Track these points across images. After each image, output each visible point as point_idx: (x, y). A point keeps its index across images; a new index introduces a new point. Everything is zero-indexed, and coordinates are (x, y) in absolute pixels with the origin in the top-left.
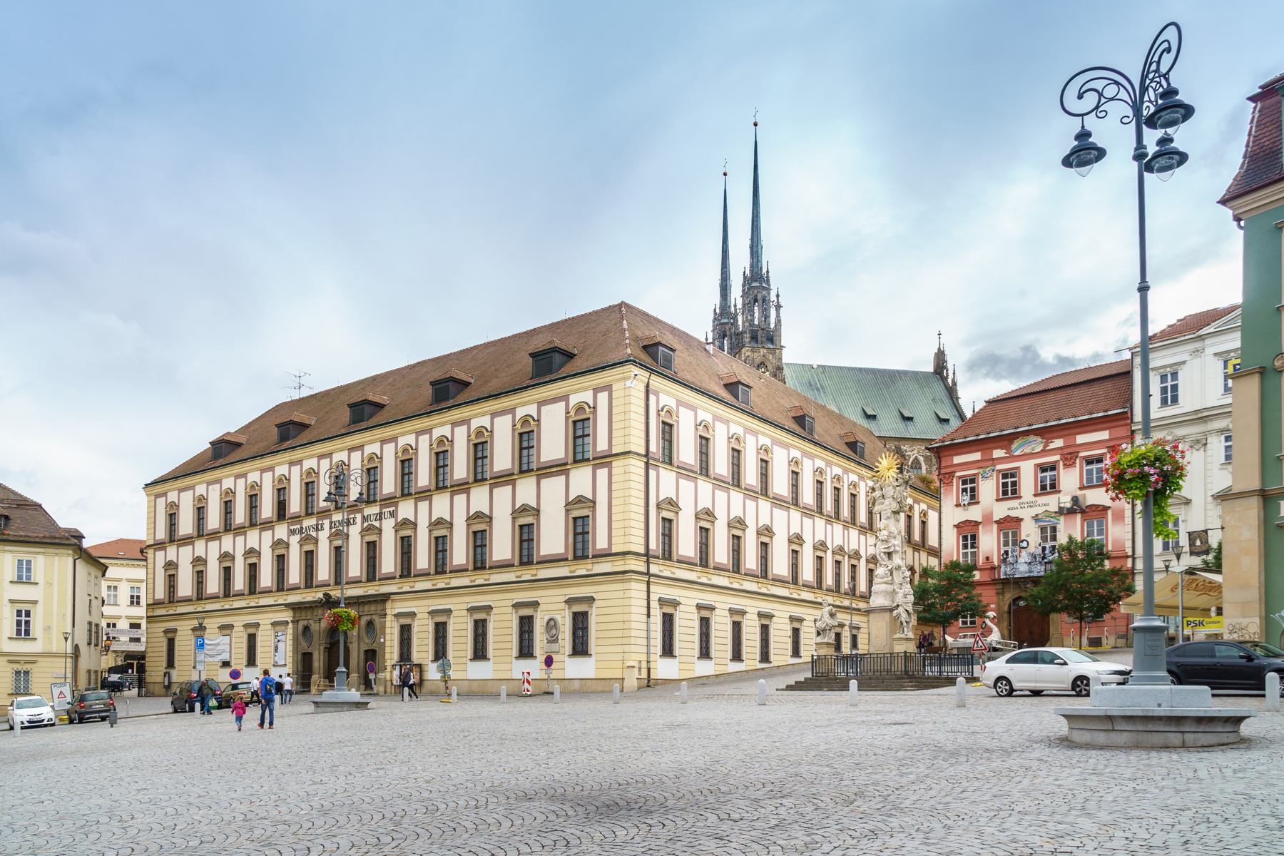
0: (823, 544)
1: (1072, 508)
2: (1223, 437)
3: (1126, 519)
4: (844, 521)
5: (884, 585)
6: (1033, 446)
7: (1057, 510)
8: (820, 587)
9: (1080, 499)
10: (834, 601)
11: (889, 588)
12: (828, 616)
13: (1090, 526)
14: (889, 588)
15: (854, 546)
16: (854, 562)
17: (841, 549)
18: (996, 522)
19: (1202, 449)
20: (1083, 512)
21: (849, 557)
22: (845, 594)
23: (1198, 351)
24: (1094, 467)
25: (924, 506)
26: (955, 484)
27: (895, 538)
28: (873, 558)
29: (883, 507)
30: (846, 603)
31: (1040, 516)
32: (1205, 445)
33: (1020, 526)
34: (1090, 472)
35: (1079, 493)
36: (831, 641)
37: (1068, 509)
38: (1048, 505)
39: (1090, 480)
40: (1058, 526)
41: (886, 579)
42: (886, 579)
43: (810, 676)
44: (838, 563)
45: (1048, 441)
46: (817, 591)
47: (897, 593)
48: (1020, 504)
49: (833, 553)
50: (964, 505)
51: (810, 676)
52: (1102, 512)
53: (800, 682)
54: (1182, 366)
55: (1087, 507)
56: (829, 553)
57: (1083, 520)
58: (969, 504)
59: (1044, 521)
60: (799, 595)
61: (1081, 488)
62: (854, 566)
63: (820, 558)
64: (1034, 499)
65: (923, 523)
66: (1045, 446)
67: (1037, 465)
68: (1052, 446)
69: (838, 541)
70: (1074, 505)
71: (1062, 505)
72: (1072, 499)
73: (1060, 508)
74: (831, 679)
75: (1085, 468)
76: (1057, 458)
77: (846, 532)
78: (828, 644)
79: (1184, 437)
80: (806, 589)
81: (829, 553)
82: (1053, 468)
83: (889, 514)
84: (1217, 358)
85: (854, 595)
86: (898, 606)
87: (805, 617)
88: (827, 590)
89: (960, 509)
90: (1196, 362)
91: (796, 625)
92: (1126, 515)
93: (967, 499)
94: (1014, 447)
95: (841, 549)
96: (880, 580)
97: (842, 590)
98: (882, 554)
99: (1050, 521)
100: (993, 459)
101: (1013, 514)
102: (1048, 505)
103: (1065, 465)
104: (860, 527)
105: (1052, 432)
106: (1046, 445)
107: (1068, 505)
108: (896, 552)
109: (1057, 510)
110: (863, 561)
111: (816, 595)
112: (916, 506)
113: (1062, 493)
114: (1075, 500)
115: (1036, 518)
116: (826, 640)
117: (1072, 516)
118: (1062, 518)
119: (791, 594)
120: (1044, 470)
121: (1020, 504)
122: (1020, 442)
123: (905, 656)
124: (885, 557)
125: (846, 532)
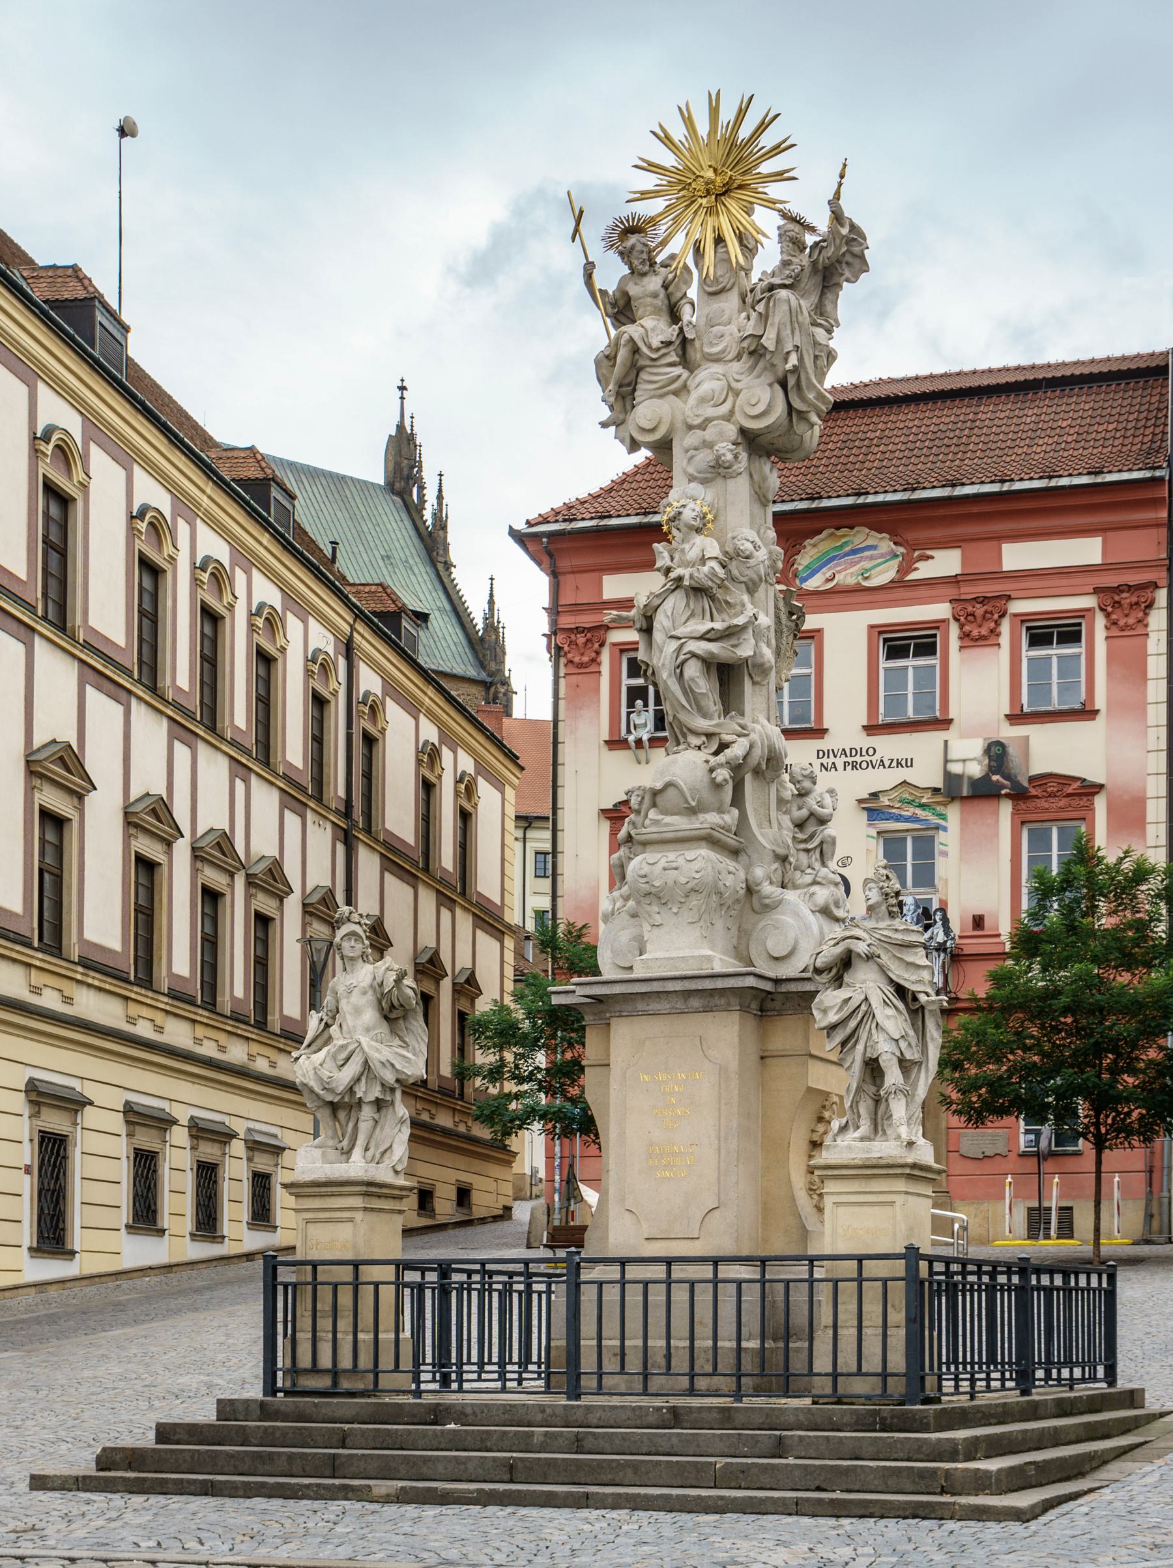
0: (161, 809)
1: (986, 778)
3: (1151, 830)
4: (233, 743)
5: (704, 853)
6: (866, 564)
7: (938, 783)
8: (146, 980)
9: (1012, 750)
10: (198, 1041)
11: (732, 875)
12: (370, 1015)
13: (1040, 841)
14: (732, 875)
15: (264, 845)
16: (263, 903)
17: (224, 842)
20: (1019, 796)
21: (251, 882)
22: (237, 1018)
24: (1054, 652)
25: (467, 764)
26: (605, 668)
27: (751, 589)
28: (323, 901)
29: (688, 408)
30: (237, 1053)
31: (885, 800)
34: (1040, 668)
35: (1009, 733)
36: (383, 1174)
37: (974, 783)
38: (909, 763)
39: (1040, 688)
40: (941, 837)
41: (712, 818)
42: (712, 818)
43: (255, 1392)
44: (211, 897)
45: (916, 551)
46: (135, 992)
47: (768, 908)
48: (820, 754)
49: (198, 855)
50: (639, 743)
51: (255, 1392)
52: (1076, 802)
53: (194, 1432)
55: (1032, 779)
56: (182, 849)
57: (1019, 822)
58: (655, 742)
59: (899, 818)
60: (68, 1000)
61: (1017, 717)
62: (263, 921)
63: (146, 866)
64: (865, 741)
65: (465, 817)
66: (904, 569)
68: (924, 570)
69: (213, 816)
70: (992, 770)
71: (955, 768)
72: (987, 751)
73: (948, 776)
74: (396, 1414)
75: (1027, 653)
76: (940, 610)
77: (240, 785)
78: (371, 1189)
80: (95, 979)
81: (182, 849)
82: (927, 648)
83: (725, 449)
85: (261, 1024)
86: (846, 962)
87: (90, 1091)
88: (174, 995)
89: (621, 757)
91: (55, 1122)
92: (1150, 817)
93: (644, 719)
95: (224, 842)
96: (680, 823)
97: (225, 1004)
99: (914, 819)
102: (909, 763)
103: (964, 636)
104: (285, 777)
105: (930, 522)
106: (906, 567)
107: (976, 770)
108: (754, 668)
109: (938, 783)
110: (293, 905)
111: (134, 1010)
112: (446, 754)
113: (953, 727)
114: (996, 753)
115: (872, 807)
116: (357, 1167)
117: (985, 806)
118: (954, 813)
119: (36, 990)
120: (896, 651)
121: (820, 754)
123: (913, 1281)
124: (705, 686)
125: (239, 785)
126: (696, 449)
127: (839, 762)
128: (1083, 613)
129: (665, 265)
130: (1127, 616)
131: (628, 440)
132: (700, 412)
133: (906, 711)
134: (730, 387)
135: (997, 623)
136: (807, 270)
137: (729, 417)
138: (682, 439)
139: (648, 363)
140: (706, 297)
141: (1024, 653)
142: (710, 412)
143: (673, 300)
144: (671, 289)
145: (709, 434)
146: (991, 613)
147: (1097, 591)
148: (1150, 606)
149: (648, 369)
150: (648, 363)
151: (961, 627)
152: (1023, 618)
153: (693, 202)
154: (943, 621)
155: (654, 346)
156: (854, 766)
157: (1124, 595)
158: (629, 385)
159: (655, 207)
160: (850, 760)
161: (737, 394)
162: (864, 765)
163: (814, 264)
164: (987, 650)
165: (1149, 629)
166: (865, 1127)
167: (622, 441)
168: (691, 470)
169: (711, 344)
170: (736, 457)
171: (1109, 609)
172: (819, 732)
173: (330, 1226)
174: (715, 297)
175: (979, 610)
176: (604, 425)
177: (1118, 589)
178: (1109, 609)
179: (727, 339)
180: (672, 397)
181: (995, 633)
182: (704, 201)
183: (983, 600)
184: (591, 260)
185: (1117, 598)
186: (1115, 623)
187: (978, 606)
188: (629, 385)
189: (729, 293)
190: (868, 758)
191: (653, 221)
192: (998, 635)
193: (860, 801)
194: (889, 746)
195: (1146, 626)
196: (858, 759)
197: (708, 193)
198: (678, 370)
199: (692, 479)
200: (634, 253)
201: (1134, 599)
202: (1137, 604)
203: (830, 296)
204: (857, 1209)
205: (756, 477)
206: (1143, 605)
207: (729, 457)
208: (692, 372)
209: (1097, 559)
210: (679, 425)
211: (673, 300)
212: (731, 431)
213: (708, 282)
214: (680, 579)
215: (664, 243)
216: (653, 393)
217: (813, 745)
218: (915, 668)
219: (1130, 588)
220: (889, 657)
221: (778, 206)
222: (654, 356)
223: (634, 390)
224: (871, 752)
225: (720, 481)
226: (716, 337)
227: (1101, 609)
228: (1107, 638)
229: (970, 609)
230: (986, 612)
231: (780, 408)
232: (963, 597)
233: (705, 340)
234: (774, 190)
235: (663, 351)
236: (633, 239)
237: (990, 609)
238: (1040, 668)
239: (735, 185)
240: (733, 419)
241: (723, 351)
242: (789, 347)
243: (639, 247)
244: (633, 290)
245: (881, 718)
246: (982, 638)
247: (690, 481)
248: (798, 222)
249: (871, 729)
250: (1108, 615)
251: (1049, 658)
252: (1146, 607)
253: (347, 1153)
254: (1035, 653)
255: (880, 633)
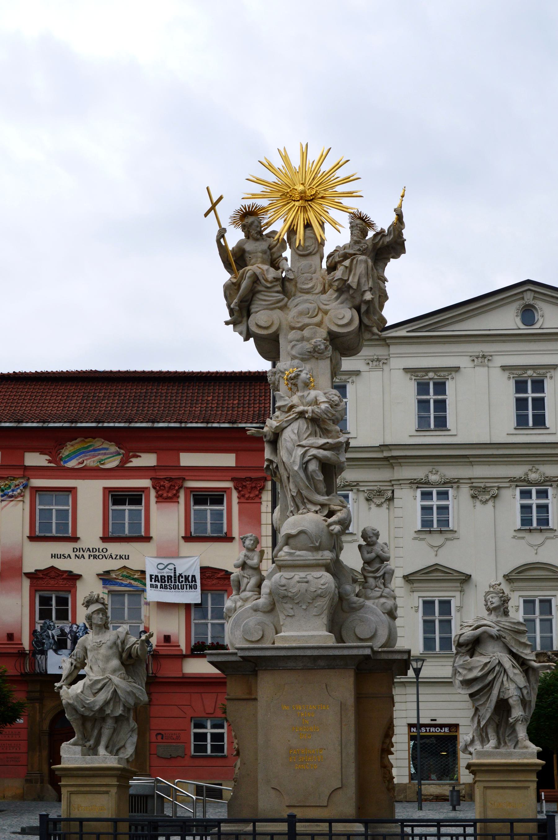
2: (419, 492)
18: (28, 575)
19: (385, 506)
23: (378, 360)
32: (391, 499)
33: (75, 587)
54: (354, 378)
64: (101, 545)
67: (107, 491)
79: (357, 483)
84: (409, 376)
90: (376, 375)
94: (65, 453)
98: (313, 466)
100: (26, 468)
101: (62, 565)
122: (77, 447)
126: (297, 341)
127: (86, 555)
128: (225, 490)
129: (268, 236)
130: (250, 493)
131: (245, 332)
132: (300, 320)
133: (124, 531)
134: (319, 309)
135: (178, 491)
136: (370, 248)
137: (319, 324)
138: (286, 335)
139: (263, 289)
140: (297, 257)
141: (192, 507)
142: (307, 321)
143: (275, 256)
144: (274, 250)
145: (306, 333)
146: (174, 486)
147: (233, 480)
148: (262, 489)
149: (263, 293)
150: (263, 289)
151: (157, 492)
152: (192, 490)
153: (288, 203)
154: (146, 488)
155: (270, 280)
156: (95, 557)
157: (248, 483)
158: (246, 301)
159: (264, 203)
160: (92, 554)
161: (326, 313)
162: (101, 557)
163: (375, 245)
164: (172, 504)
165: (262, 500)
166: (503, 744)
167: (241, 333)
168: (294, 352)
169: (303, 283)
170: (326, 348)
171: (240, 489)
172: (75, 539)
173: (90, 796)
174: (304, 258)
175: (167, 484)
176: (227, 323)
177: (246, 479)
178: (240, 489)
179: (314, 281)
180: (278, 311)
181: (176, 496)
182: (297, 204)
183: (170, 479)
184: (223, 227)
185: (244, 484)
186: (243, 496)
187: (167, 482)
188: (246, 301)
189: (314, 257)
190: (103, 554)
191: (264, 210)
192: (178, 497)
193: (98, 575)
194: (115, 548)
195: (261, 498)
196: (97, 553)
197: (301, 198)
198: (281, 296)
199: (294, 358)
200: (253, 227)
201: (254, 485)
202: (255, 487)
203: (381, 264)
204: (501, 791)
205: (334, 361)
206: (259, 488)
207: (323, 347)
208: (289, 299)
209: (233, 464)
210: (284, 326)
211: (275, 256)
212: (322, 333)
213: (301, 248)
214: (301, 414)
215: (269, 224)
216: (265, 307)
217: (71, 545)
218: (129, 510)
219: (251, 479)
220: (114, 504)
221: (350, 211)
222: (269, 285)
223: (250, 304)
224: (105, 550)
225: (313, 360)
226: (306, 279)
227: (236, 489)
228: (239, 503)
229: (162, 483)
230: (171, 485)
231: (356, 322)
232: (157, 477)
233: (299, 281)
234: (346, 202)
235: (275, 283)
236: (250, 219)
237: (173, 484)
238: (201, 515)
239: (319, 196)
240: (323, 326)
241: (312, 288)
242: (366, 288)
243: (256, 223)
244: (249, 247)
245: (110, 534)
246: (171, 498)
247: (292, 359)
248: (364, 220)
249: (105, 539)
250: (239, 492)
251: (206, 510)
252: (260, 489)
253: (93, 751)
254: (197, 507)
255: (110, 492)
